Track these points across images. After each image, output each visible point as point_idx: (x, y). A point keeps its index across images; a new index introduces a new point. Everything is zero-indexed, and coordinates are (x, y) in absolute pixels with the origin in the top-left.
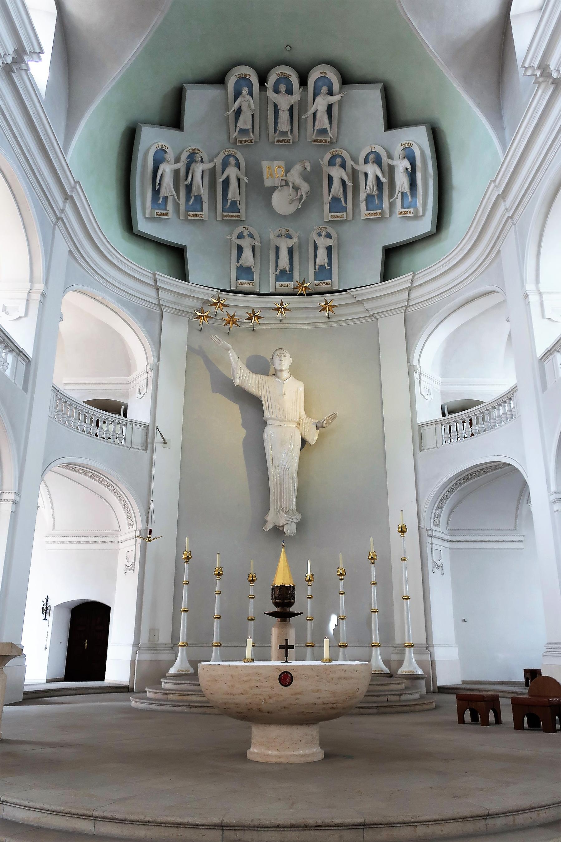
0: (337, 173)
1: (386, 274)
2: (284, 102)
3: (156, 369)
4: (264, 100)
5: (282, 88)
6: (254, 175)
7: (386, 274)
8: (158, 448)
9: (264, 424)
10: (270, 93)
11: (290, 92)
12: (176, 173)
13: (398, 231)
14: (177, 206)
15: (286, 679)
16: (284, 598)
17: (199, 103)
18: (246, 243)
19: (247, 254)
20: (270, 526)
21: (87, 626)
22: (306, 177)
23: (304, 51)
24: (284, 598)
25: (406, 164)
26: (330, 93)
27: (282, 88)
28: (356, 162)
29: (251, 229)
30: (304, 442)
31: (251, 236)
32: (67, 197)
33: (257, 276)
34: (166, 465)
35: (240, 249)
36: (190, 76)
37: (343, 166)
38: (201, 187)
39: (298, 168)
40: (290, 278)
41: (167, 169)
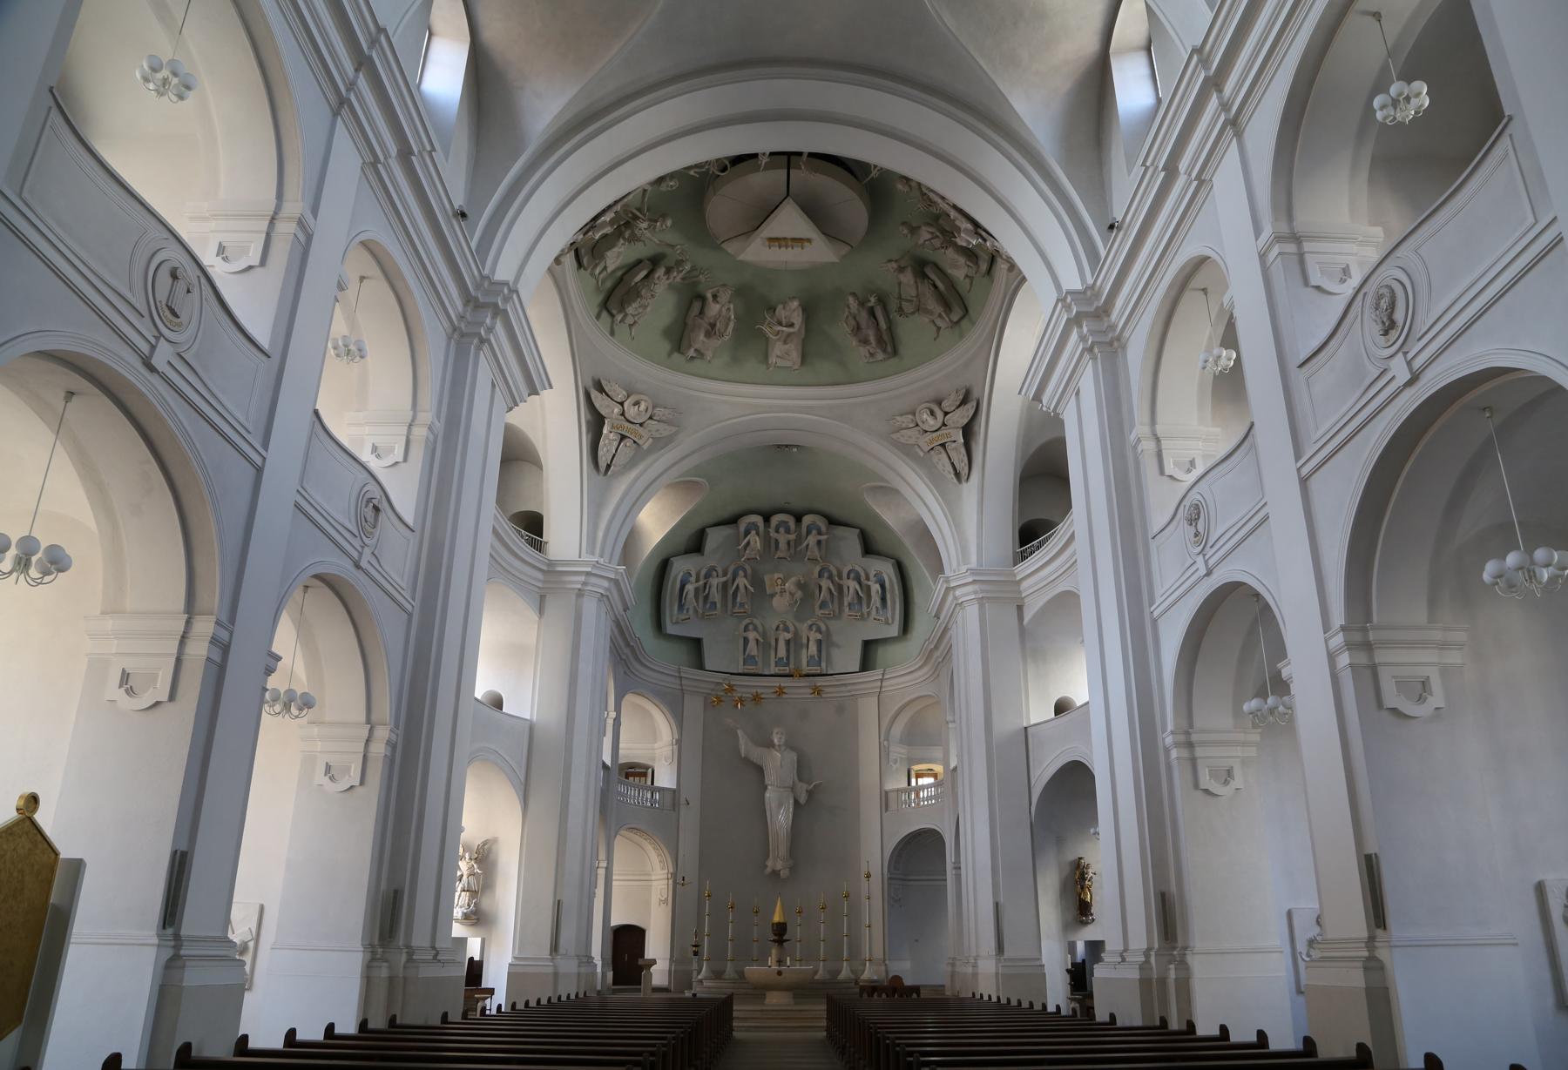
0: (825, 583)
1: (866, 664)
2: (783, 538)
3: (679, 742)
4: (767, 533)
5: (782, 530)
6: (757, 581)
7: (866, 664)
8: (683, 809)
9: (765, 788)
10: (773, 534)
11: (788, 531)
12: (697, 590)
13: (873, 631)
14: (696, 611)
15: (780, 973)
16: (780, 930)
17: (715, 538)
18: (752, 635)
19: (752, 644)
20: (769, 870)
21: (627, 941)
22: (800, 586)
23: (797, 503)
24: (780, 930)
25: (878, 586)
26: (820, 533)
27: (782, 530)
28: (840, 577)
29: (756, 621)
30: (796, 802)
31: (755, 629)
32: (628, 645)
33: (759, 660)
34: (689, 819)
35: (746, 640)
36: (712, 520)
37: (830, 577)
38: (716, 596)
39: (793, 579)
40: (788, 664)
41: (690, 588)
